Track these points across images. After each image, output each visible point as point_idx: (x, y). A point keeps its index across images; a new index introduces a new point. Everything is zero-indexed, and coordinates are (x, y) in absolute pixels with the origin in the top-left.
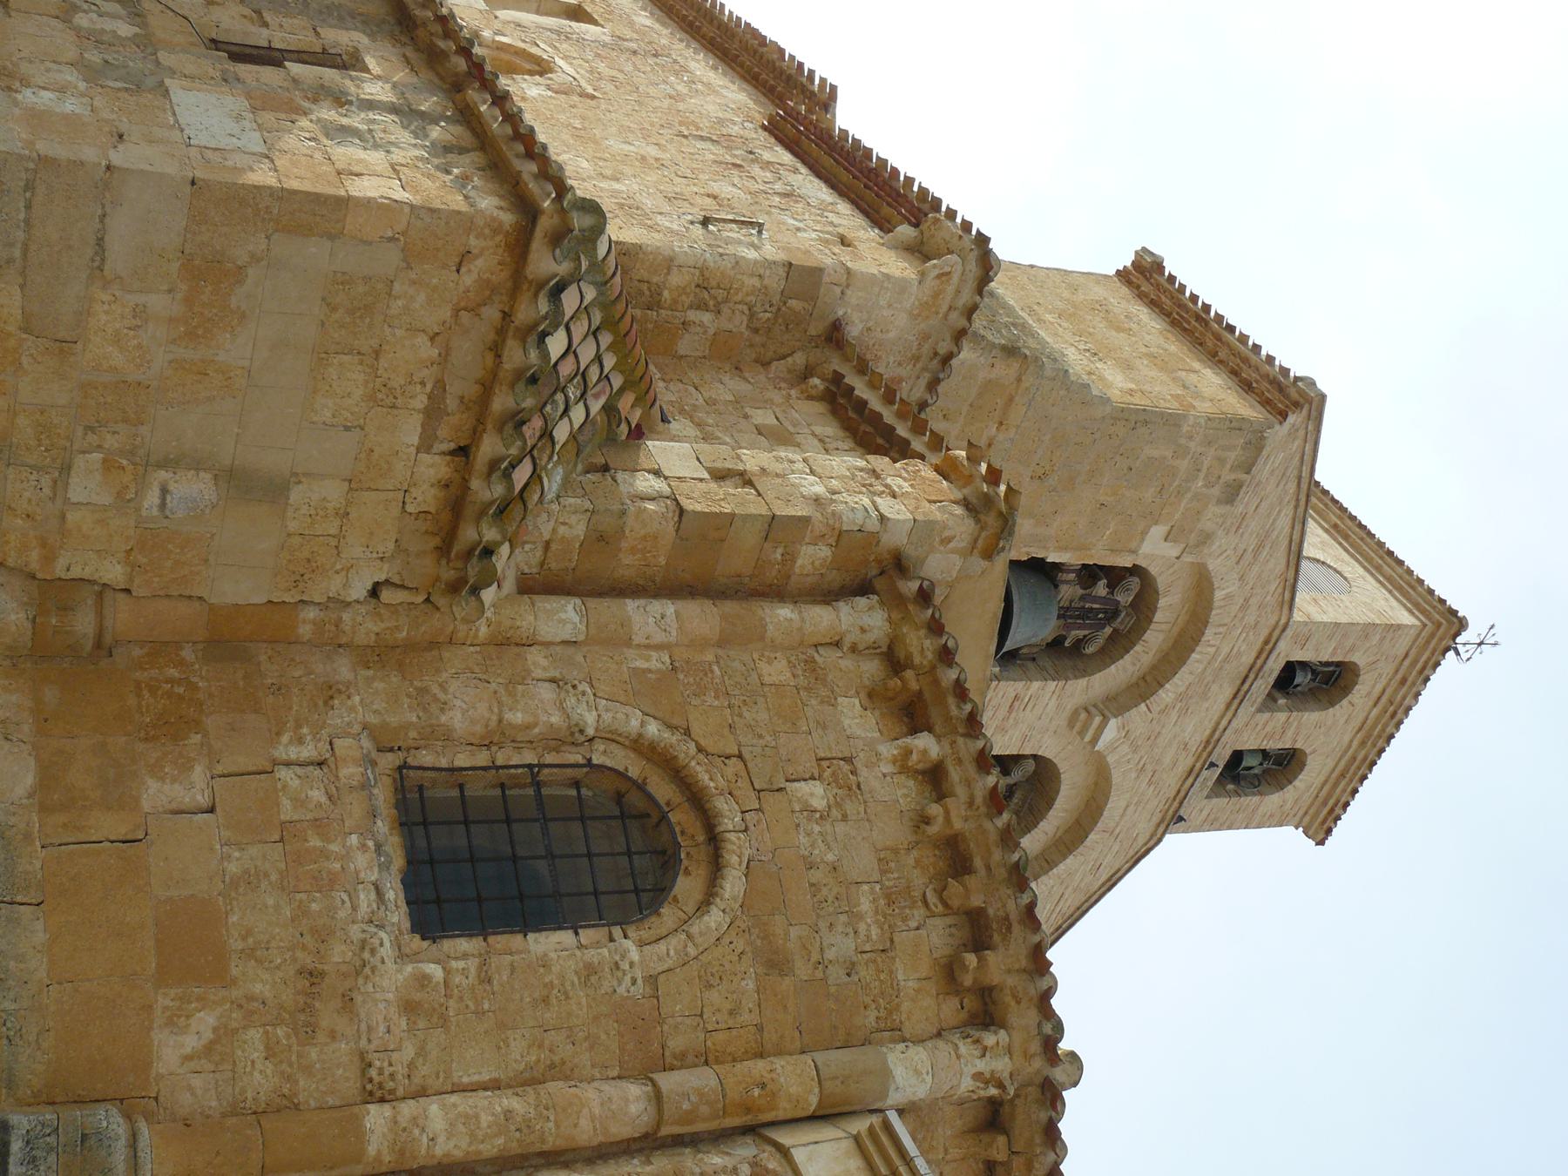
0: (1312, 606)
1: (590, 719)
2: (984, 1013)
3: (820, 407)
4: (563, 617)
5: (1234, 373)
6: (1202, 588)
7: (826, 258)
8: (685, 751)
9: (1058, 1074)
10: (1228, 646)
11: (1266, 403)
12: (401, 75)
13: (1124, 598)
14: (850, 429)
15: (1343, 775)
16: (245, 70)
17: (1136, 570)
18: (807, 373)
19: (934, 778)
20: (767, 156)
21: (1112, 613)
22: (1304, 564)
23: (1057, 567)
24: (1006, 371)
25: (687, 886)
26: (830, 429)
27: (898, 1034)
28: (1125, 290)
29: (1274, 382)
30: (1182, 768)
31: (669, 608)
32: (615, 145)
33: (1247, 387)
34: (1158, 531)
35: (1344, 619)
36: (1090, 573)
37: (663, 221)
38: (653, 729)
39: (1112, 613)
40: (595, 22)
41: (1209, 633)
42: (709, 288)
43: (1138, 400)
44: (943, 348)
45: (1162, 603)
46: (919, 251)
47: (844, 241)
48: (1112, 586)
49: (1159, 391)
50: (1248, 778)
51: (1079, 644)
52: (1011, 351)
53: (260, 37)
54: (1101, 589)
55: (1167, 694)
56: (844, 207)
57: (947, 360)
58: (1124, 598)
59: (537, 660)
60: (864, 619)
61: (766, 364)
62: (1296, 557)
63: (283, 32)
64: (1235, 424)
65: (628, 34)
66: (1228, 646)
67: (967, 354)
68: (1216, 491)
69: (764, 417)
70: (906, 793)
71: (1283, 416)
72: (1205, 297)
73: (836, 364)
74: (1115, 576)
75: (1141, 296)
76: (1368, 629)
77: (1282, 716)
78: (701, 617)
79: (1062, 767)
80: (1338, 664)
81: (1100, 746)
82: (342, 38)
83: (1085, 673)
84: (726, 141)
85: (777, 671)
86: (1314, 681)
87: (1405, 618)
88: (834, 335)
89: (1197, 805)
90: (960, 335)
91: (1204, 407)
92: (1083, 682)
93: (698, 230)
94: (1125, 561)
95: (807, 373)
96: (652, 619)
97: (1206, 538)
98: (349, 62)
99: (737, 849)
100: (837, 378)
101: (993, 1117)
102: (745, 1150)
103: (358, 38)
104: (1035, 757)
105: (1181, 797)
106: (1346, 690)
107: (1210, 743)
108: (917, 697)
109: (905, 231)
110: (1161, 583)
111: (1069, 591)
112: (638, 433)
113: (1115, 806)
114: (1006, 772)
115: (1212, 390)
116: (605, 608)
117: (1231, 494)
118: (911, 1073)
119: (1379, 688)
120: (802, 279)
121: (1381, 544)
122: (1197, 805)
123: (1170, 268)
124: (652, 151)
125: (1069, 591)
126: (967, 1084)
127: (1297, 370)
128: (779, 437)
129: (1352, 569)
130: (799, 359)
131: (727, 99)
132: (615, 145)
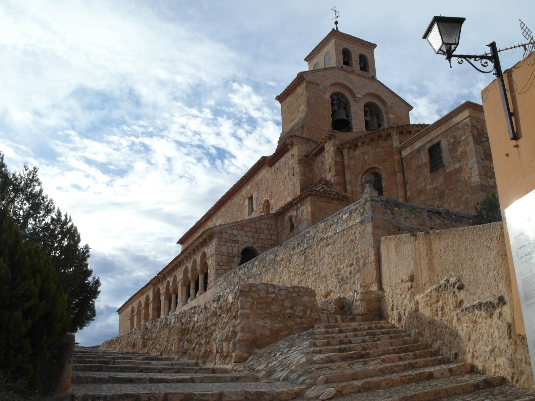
0: (333, 63)
1: (360, 183)
2: (389, 135)
3: (317, 158)
4: (349, 187)
5: (297, 85)
6: (333, 85)
7: (296, 158)
8: (362, 172)
9: (395, 126)
10: (342, 77)
11: (302, 81)
12: (292, 211)
13: (335, 97)
14: (320, 154)
15: (363, 45)
16: (295, 226)
17: (331, 97)
18: (312, 159)
19: (363, 143)
20: (278, 167)
21: (339, 99)
22: (326, 67)
23: (332, 111)
24: (305, 128)
25: (377, 171)
26: (320, 156)
27: (392, 145)
28: (284, 102)
29: (298, 80)
30: (363, 79)
31: (347, 176)
32: (281, 188)
33: (299, 84)
34: (325, 96)
35: (335, 55)
36: (333, 105)
37: (295, 181)
38: (360, 176)
39: (339, 99)
40: (252, 195)
41: (340, 82)
42: (303, 174)
43: (306, 104)
44: (305, 140)
45: (336, 91)
46: (292, 144)
47: (293, 155)
48: (334, 100)
49: (303, 100)
50: (366, 64)
51: (344, 104)
52: (303, 128)
53: (289, 227)
54: (335, 102)
55: (351, 86)
56: (286, 155)
57: (307, 139)
58: (335, 97)
59: (354, 190)
60: (345, 152)
61: (311, 165)
62: (325, 69)
63: (288, 225)
64: (307, 87)
65: (253, 189)
66: (342, 77)
67: (304, 135)
68: (317, 88)
69: (320, 165)
70: (365, 146)
71: (304, 79)
72: (284, 89)
73: (311, 155)
74: (332, 100)
75: (284, 99)
76: (336, 49)
77: (353, 62)
78: (347, 172)
79: (366, 102)
80: (343, 51)
81: (361, 97)
82: (287, 218)
83: (349, 102)
84: (276, 173)
85: (353, 162)
86: (346, 54)
87: (333, 41)
88: (306, 156)
89: (370, 75)
90: (303, 138)
91: (305, 93)
92: (351, 102)
93: (295, 176)
94: (330, 99)
95: (312, 159)
96: (348, 177)
97: (325, 87)
98: (291, 218)
99: (373, 166)
100: (313, 155)
101: (401, 133)
102: (404, 163)
103: (287, 218)
104: (365, 106)
105: (369, 78)
106: (347, 49)
107: (359, 75)
108: (354, 145)
109: (289, 147)
110: (332, 92)
111: (336, 108)
112: (326, 181)
113: (372, 91)
114: (367, 112)
115: (301, 89)
116: (347, 183)
117: (318, 85)
118: (396, 144)
119: (346, 43)
120: (300, 161)
121: (320, 44)
122: (370, 75)
123: (279, 95)
124: (281, 183)
125: (336, 108)
126: (397, 137)
127: (296, 76)
128: (322, 163)
129: (325, 50)
130: (310, 161)
131: (265, 173)
132: (281, 188)
